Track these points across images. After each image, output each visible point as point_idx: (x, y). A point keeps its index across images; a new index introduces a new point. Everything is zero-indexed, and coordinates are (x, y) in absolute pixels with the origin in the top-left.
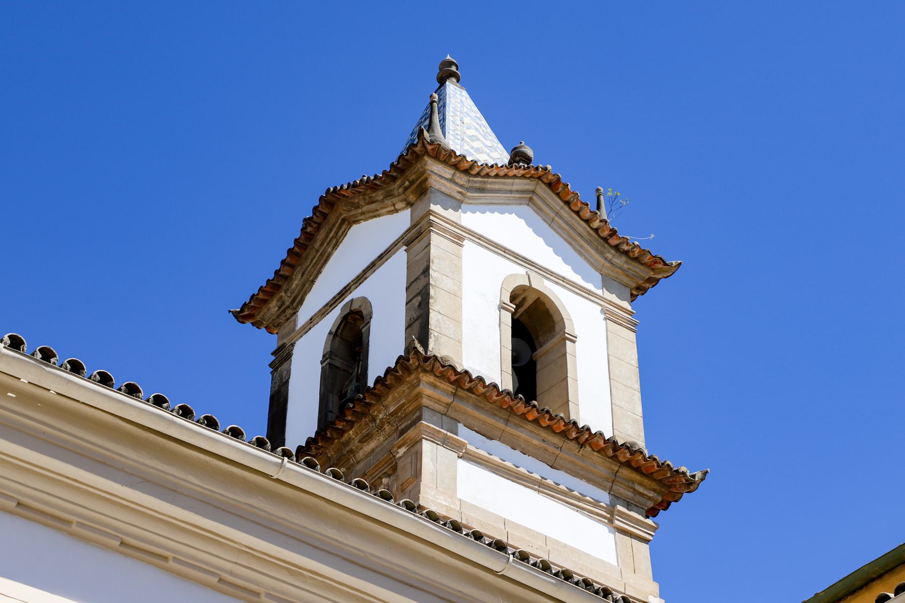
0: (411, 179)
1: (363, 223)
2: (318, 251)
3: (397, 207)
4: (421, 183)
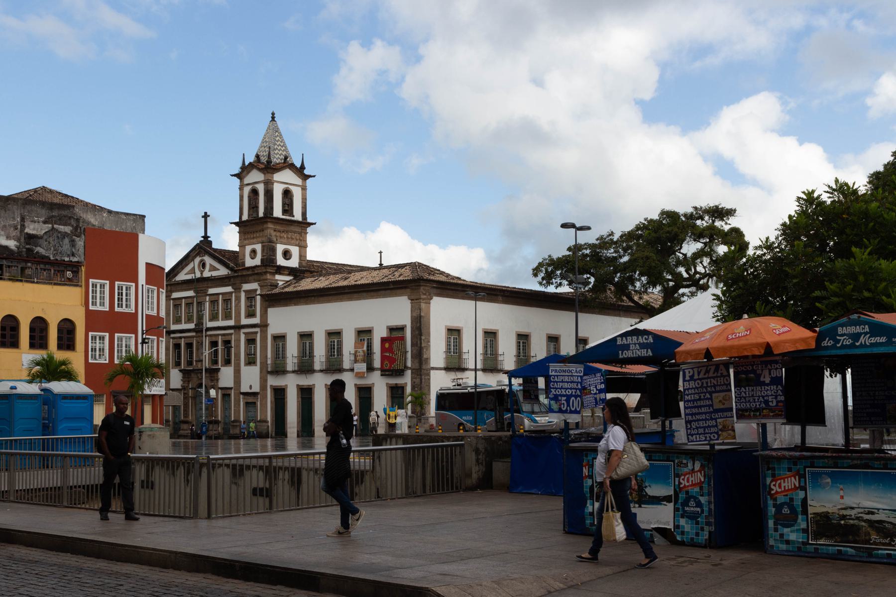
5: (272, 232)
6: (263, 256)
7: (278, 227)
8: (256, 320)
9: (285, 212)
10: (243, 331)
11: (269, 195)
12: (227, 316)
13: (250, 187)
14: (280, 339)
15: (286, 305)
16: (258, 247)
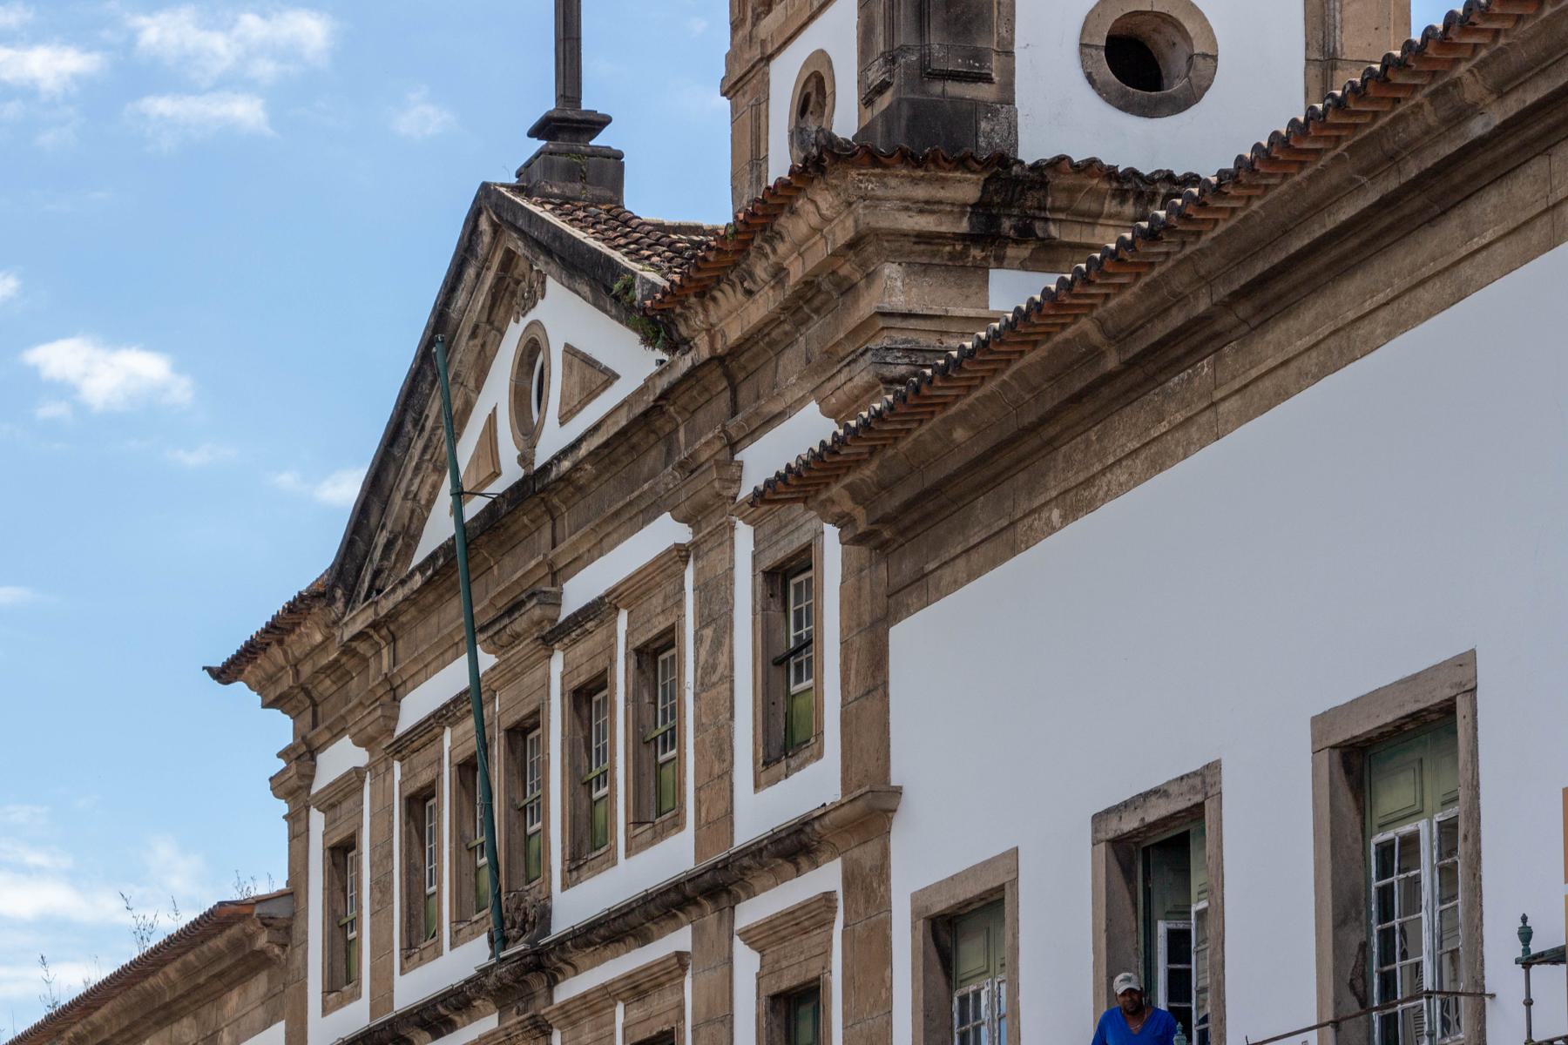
8: (816, 785)
10: (753, 911)
12: (655, 811)
14: (967, 924)
15: (1007, 541)
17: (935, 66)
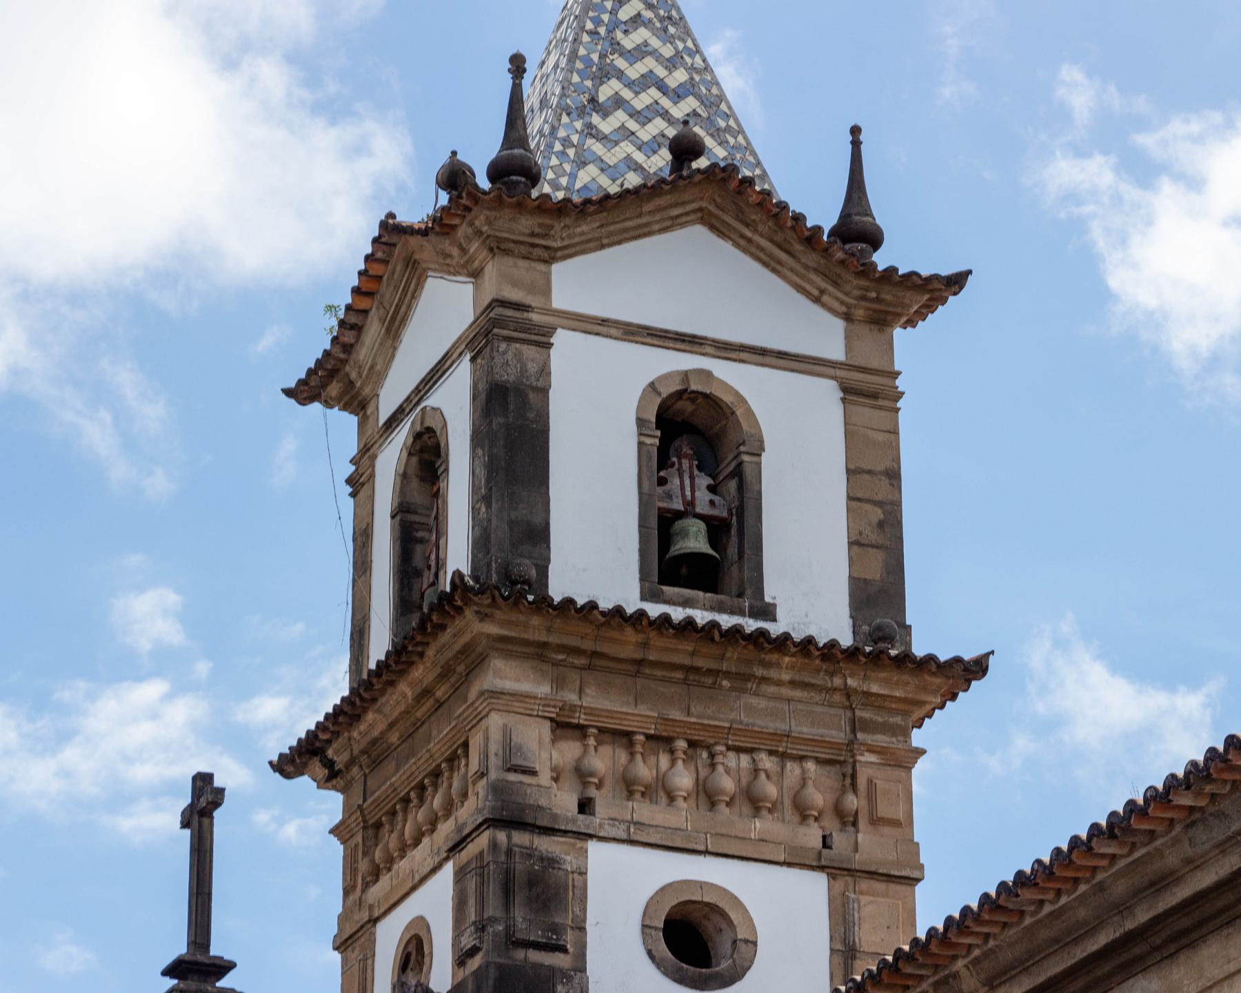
0: (883, 296)
1: (727, 246)
2: (640, 215)
3: (825, 298)
4: (887, 313)
5: (533, 737)
6: (461, 960)
7: (599, 700)
9: (668, 567)
11: (516, 433)
13: (402, 436)
16: (435, 902)
17: (519, 935)
